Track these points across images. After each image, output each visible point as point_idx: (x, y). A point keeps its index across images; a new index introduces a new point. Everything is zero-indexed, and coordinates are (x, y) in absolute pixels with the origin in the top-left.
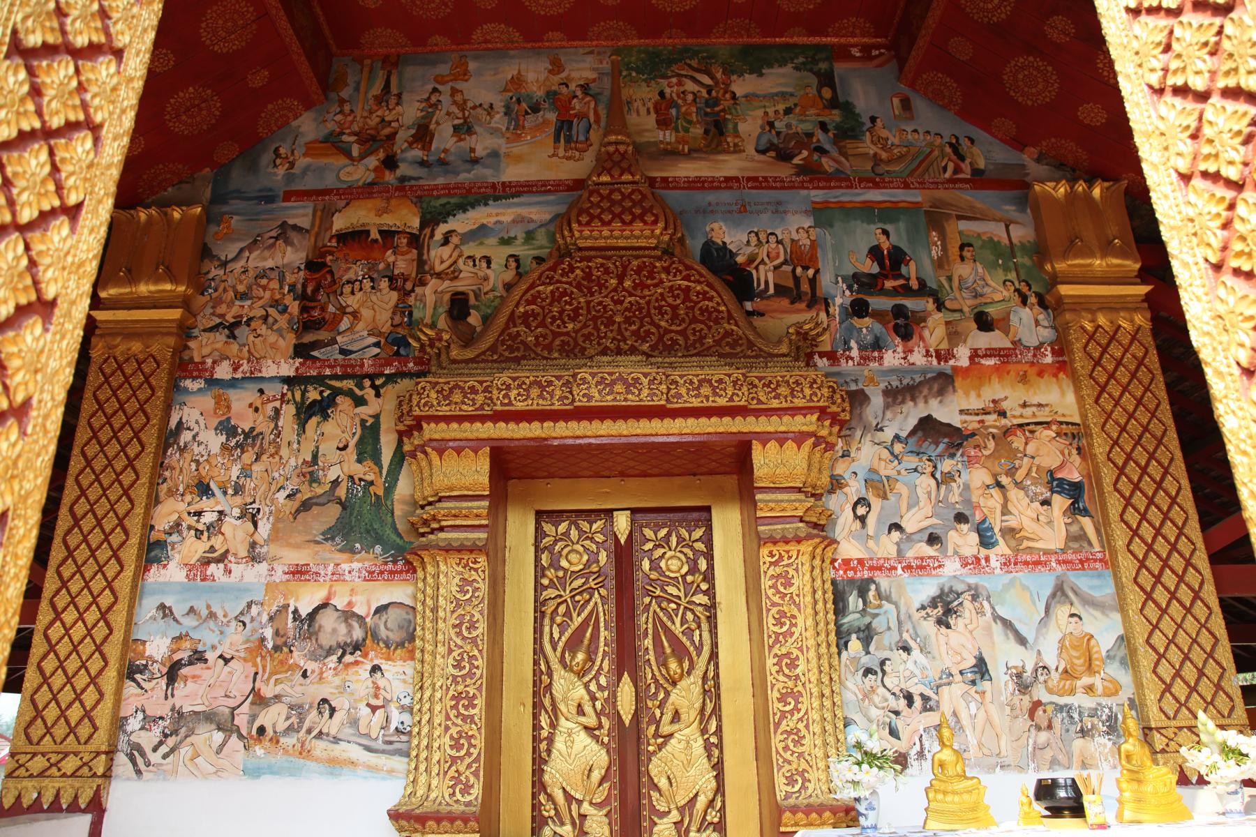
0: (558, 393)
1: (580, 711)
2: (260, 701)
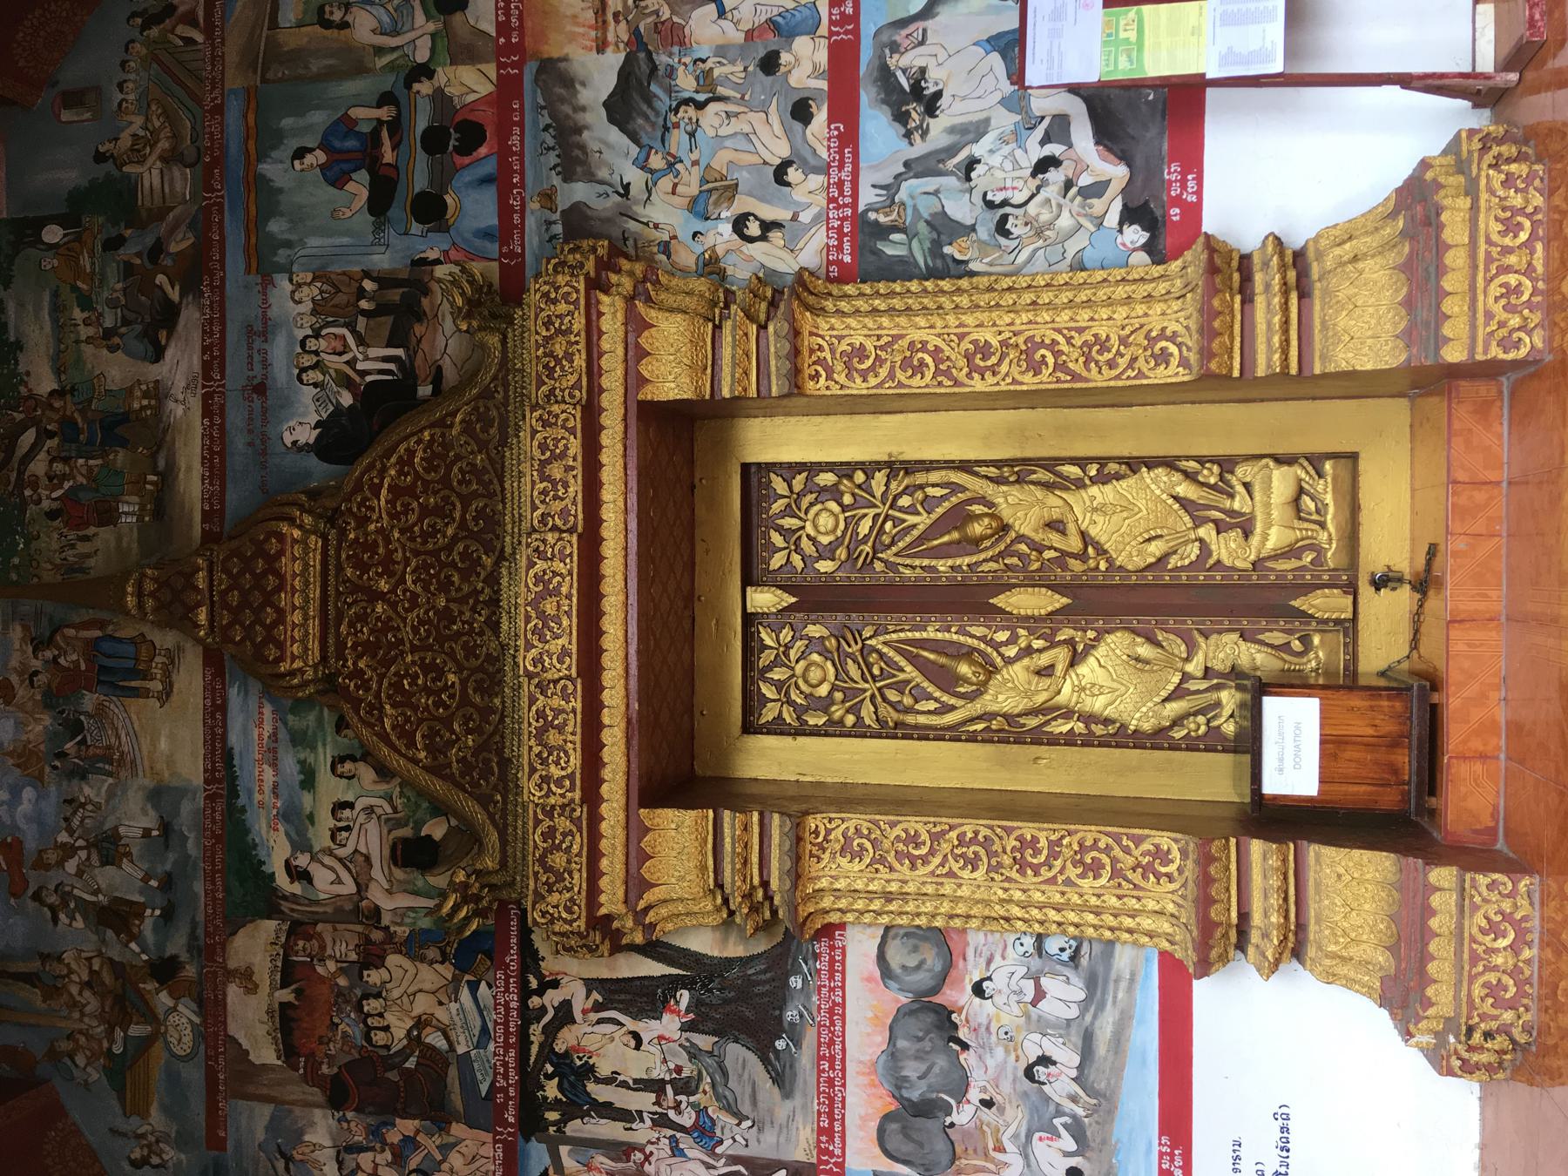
0: (557, 702)
1: (1046, 672)
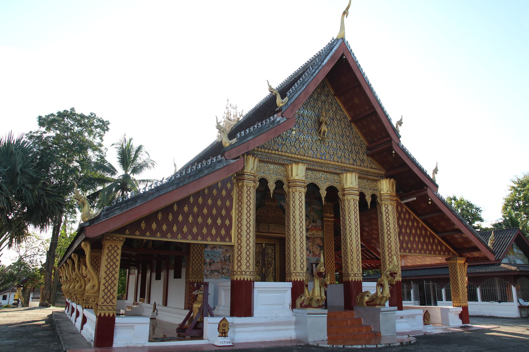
2: (223, 269)
